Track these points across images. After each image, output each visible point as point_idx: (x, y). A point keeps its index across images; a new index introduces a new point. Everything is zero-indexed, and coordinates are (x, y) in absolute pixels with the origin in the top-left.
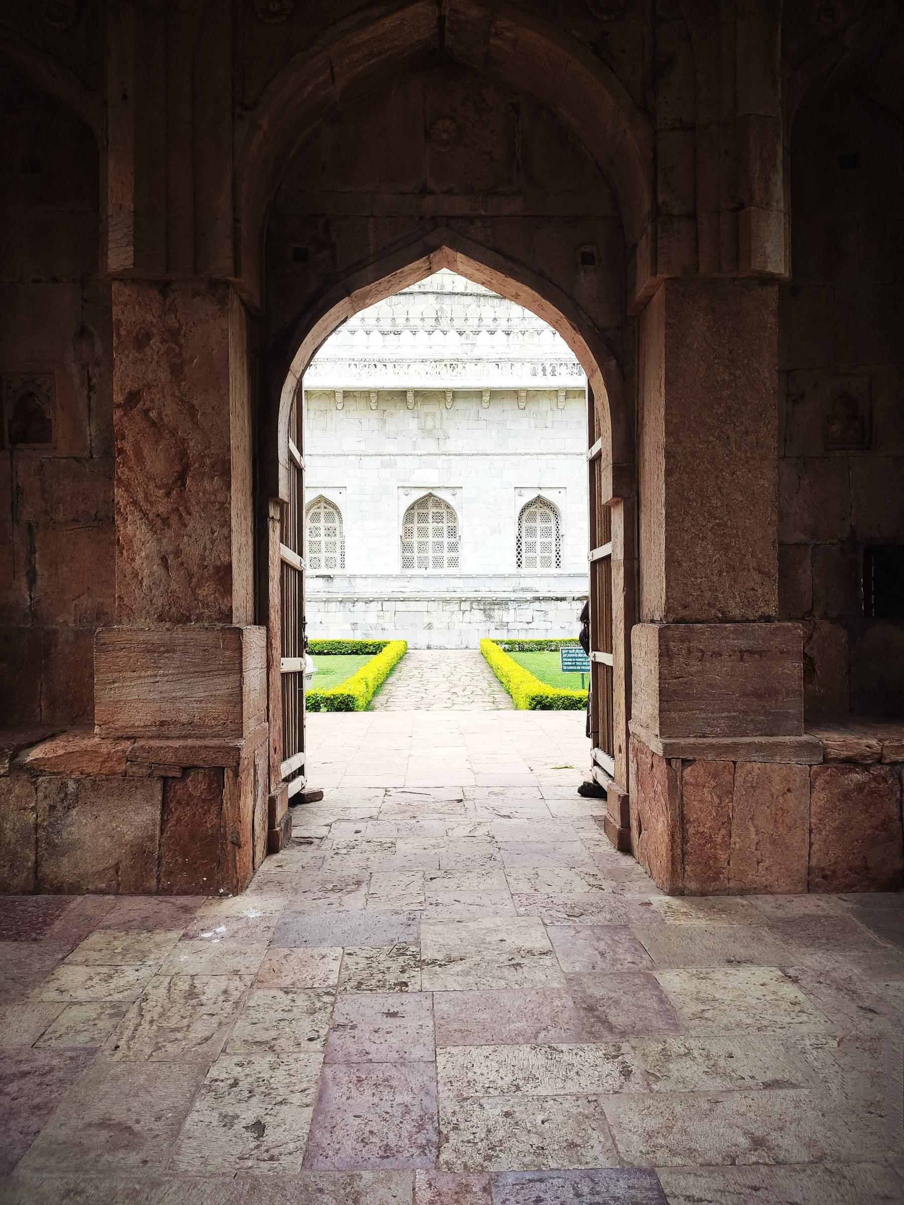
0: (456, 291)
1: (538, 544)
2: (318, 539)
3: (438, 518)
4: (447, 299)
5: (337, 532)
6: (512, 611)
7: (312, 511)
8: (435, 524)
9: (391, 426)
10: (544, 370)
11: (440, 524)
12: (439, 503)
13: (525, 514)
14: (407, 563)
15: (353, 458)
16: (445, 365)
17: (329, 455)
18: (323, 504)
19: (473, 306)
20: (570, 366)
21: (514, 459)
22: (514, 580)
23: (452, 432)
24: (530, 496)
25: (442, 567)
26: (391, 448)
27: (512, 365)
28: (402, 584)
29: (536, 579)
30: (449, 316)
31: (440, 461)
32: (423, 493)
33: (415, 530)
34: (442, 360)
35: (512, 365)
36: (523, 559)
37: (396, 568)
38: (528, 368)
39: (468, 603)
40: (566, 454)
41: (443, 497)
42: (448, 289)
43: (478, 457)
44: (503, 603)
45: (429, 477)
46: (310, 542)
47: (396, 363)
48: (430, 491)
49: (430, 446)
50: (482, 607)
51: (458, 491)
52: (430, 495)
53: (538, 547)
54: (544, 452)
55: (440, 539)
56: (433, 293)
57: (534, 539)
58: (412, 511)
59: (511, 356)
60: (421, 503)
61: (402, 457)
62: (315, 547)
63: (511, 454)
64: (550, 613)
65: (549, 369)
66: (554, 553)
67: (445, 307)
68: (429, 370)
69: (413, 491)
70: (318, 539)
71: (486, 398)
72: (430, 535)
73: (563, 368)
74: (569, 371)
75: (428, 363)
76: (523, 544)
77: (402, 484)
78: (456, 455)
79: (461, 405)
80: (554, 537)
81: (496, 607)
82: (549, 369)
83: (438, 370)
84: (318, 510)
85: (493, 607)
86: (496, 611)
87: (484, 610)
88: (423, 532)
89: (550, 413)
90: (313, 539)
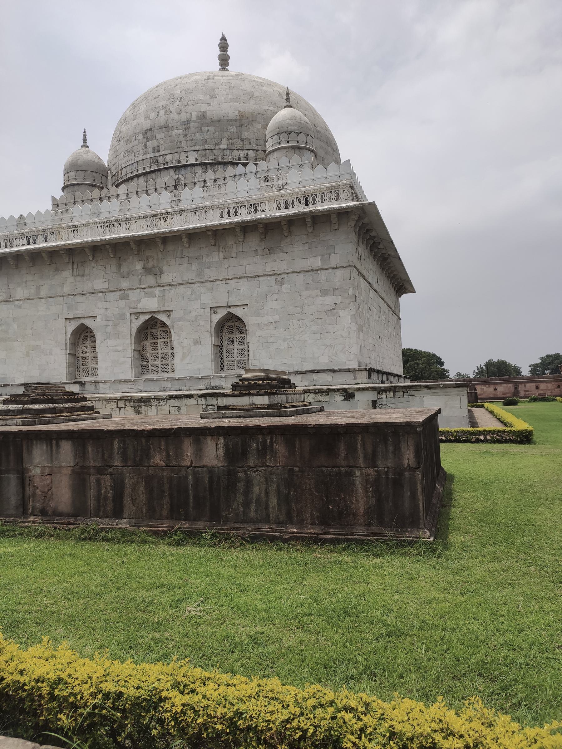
1: (235, 350)
4: (183, 171)
6: (154, 407)
7: (83, 335)
8: (162, 340)
9: (124, 269)
10: (229, 212)
11: (166, 340)
13: (225, 328)
14: (144, 370)
15: (101, 294)
16: (160, 219)
17: (86, 294)
21: (209, 285)
22: (207, 381)
23: (165, 269)
24: (222, 313)
25: (167, 372)
26: (125, 284)
27: (206, 212)
28: (130, 386)
29: (222, 379)
31: (157, 292)
32: (147, 317)
34: (157, 215)
35: (206, 212)
36: (225, 364)
37: (130, 375)
38: (217, 213)
39: (123, 402)
40: (247, 278)
41: (161, 319)
42: (183, 163)
43: (183, 286)
44: (147, 401)
45: (150, 304)
47: (127, 221)
49: (150, 280)
50: (132, 404)
51: (171, 313)
53: (235, 353)
54: (230, 277)
55: (166, 351)
57: (232, 347)
58: (147, 331)
59: (203, 205)
61: (132, 291)
62: (86, 361)
63: (205, 282)
64: (182, 408)
65: (232, 212)
67: (180, 176)
68: (149, 224)
70: (87, 355)
71: (185, 240)
73: (243, 209)
74: (247, 210)
75: (148, 219)
76: (225, 351)
77: (133, 311)
78: (167, 286)
79: (170, 247)
81: (143, 404)
82: (232, 212)
83: (154, 222)
84: (87, 334)
85: (140, 404)
86: (143, 407)
87: (134, 407)
89: (234, 246)
90: (84, 355)
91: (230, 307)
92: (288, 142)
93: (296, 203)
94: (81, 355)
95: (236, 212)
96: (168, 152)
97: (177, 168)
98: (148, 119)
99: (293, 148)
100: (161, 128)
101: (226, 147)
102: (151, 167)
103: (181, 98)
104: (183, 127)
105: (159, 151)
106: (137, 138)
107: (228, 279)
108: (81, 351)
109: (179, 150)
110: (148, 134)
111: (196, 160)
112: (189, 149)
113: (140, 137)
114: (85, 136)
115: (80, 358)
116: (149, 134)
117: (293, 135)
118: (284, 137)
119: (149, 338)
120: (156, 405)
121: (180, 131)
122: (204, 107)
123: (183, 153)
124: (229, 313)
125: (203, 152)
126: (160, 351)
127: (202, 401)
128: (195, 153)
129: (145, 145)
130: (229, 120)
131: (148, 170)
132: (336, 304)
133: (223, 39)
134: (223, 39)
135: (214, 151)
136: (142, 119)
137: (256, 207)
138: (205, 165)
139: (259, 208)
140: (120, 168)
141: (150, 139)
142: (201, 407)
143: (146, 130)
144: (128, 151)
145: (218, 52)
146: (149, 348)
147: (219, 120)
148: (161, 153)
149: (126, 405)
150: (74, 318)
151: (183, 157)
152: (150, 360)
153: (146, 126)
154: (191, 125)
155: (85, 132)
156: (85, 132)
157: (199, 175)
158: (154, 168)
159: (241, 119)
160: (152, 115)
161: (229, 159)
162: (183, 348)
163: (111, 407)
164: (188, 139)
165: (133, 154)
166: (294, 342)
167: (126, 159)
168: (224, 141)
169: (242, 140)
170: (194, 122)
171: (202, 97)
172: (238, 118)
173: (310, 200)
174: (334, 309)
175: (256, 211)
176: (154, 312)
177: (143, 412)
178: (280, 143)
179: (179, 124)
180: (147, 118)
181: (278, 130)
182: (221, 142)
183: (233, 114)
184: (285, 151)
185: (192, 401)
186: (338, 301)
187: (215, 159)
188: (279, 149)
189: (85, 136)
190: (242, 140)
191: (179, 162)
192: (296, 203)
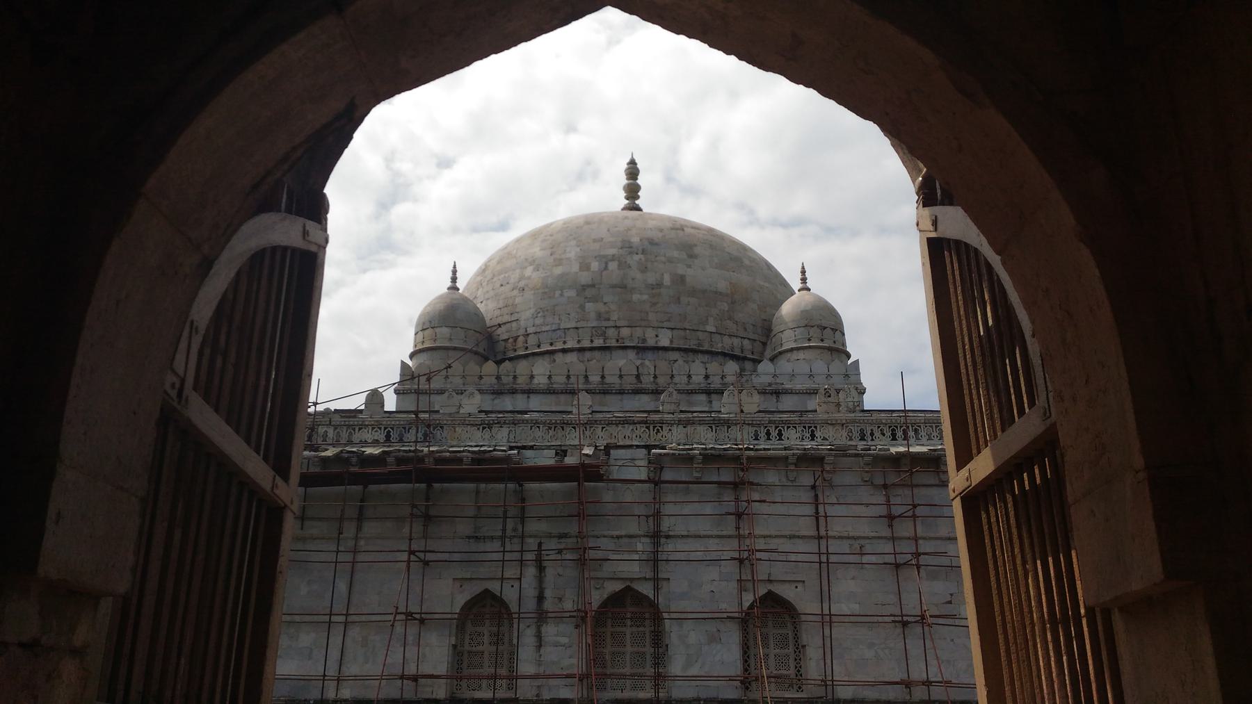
4: (650, 355)
8: (634, 629)
10: (768, 434)
11: (641, 629)
12: (640, 599)
19: (680, 362)
20: (799, 429)
30: (652, 372)
32: (618, 586)
42: (651, 342)
43: (690, 540)
46: (469, 652)
48: (628, 583)
52: (628, 588)
56: (633, 347)
60: (616, 600)
66: (792, 672)
67: (647, 362)
69: (607, 584)
70: (480, 648)
74: (798, 435)
80: (791, 649)
82: (774, 433)
91: (770, 581)
93: (877, 434)
94: (467, 647)
95: (780, 434)
97: (641, 349)
99: (830, 349)
100: (614, 286)
101: (713, 330)
105: (608, 320)
106: (566, 294)
107: (770, 536)
108: (467, 641)
109: (643, 323)
110: (589, 291)
111: (671, 342)
113: (572, 293)
114: (454, 272)
116: (589, 293)
117: (828, 331)
118: (815, 332)
121: (645, 297)
122: (681, 269)
123: (650, 330)
124: (770, 593)
125: (682, 333)
126: (629, 649)
128: (669, 333)
129: (582, 307)
131: (586, 344)
133: (633, 163)
134: (633, 163)
135: (699, 334)
136: (575, 268)
138: (686, 351)
139: (818, 434)
140: (522, 332)
141: (594, 299)
145: (624, 181)
146: (609, 640)
147: (704, 291)
150: (471, 579)
153: (585, 278)
158: (598, 342)
160: (595, 266)
161: (718, 347)
165: (557, 318)
167: (538, 321)
168: (711, 320)
169: (736, 323)
171: (676, 254)
173: (899, 434)
174: (950, 602)
175: (813, 437)
176: (632, 580)
180: (585, 267)
183: (722, 286)
184: (818, 351)
187: (699, 345)
188: (810, 347)
190: (736, 323)
191: (644, 340)
192: (877, 434)
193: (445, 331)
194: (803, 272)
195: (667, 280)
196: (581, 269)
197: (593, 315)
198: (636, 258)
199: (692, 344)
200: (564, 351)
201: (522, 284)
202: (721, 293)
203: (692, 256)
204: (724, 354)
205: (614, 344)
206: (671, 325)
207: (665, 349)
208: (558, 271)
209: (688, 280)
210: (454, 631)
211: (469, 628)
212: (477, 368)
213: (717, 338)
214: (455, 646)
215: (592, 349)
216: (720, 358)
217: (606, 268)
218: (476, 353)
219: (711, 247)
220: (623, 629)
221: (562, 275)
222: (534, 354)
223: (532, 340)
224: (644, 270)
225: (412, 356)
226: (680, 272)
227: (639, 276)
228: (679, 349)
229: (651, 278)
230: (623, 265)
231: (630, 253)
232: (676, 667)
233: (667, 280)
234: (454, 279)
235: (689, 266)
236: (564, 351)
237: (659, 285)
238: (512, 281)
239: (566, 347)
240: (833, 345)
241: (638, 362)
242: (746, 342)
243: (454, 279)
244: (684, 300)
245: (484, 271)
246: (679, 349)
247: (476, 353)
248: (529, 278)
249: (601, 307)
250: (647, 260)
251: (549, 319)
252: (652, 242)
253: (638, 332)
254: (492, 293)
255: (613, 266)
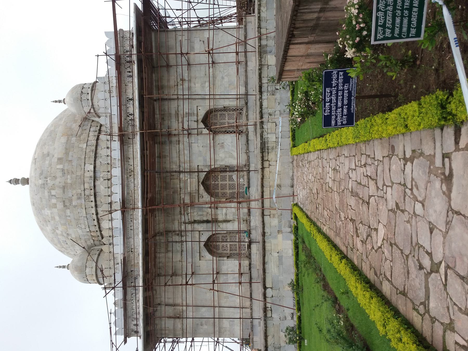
0: (93, 169)
2: (228, 246)
3: (216, 178)
4: (98, 174)
5: (225, 235)
8: (219, 180)
11: (219, 177)
12: (207, 178)
18: (210, 244)
19: (100, 160)
30: (106, 173)
32: (202, 188)
33: (222, 191)
42: (92, 174)
46: (230, 251)
48: (200, 183)
52: (203, 183)
56: (94, 182)
60: (207, 189)
62: (233, 248)
64: (269, 112)
67: (101, 175)
70: (228, 246)
72: (225, 182)
76: (229, 130)
88: (223, 187)
92: (88, 94)
94: (228, 252)
96: (82, 186)
98: (56, 204)
99: (92, 90)
102: (92, 201)
103: (45, 178)
104: (66, 174)
106: (69, 214)
108: (225, 252)
109: (82, 177)
111: (91, 164)
112: (83, 170)
113: (68, 211)
114: (60, 267)
115: (231, 252)
117: (83, 91)
119: (216, 191)
120: (268, 134)
121: (69, 176)
122: (55, 160)
125: (86, 159)
126: (227, 182)
127: (265, 96)
128: (86, 165)
129: (75, 206)
130: (67, 143)
131: (93, 204)
132: (200, 41)
135: (87, 151)
136: (55, 210)
137: (129, 99)
138: (95, 157)
140: (89, 234)
141: (71, 201)
142: (270, 97)
143: (64, 206)
144: (77, 224)
146: (225, 191)
147: (66, 149)
148: (83, 193)
149: (267, 160)
151: (87, 174)
152: (234, 191)
154: (66, 168)
155: (57, 267)
156: (57, 267)
157: (103, 160)
158: (92, 198)
159: (68, 135)
160: (54, 201)
161: (95, 142)
162: (226, 157)
163: (269, 173)
164: (75, 170)
166: (225, 71)
167: (83, 227)
168: (81, 146)
170: (64, 166)
171: (47, 162)
172: (66, 137)
174: (204, 42)
176: (199, 182)
177: (272, 145)
178: (88, 100)
179: (63, 178)
180: (55, 206)
181: (79, 101)
182: (82, 148)
183: (63, 140)
185: (265, 104)
186: (198, 39)
189: (60, 267)
191: (91, 177)
193: (88, 270)
194: (56, 102)
195: (60, 166)
196: (56, 207)
197: (79, 201)
198: (49, 181)
199: (93, 155)
200: (97, 214)
201: (65, 235)
202: (67, 141)
203: (48, 155)
204: (98, 139)
205: (93, 191)
206: (83, 164)
207: (95, 167)
208: (57, 218)
209: (59, 157)
210: (222, 258)
211: (220, 251)
212: (106, 254)
213: (89, 143)
214: (228, 257)
215: (96, 201)
216: (99, 141)
217: (55, 196)
218: (99, 255)
219: (45, 144)
220: (220, 185)
221: (60, 217)
222: (99, 228)
223: (93, 229)
224: (55, 177)
225: (101, 284)
226: (56, 160)
227: (58, 180)
228: (95, 161)
229: (59, 174)
230: (53, 188)
231: (47, 184)
232: (234, 162)
233: (60, 166)
234: (64, 267)
235: (53, 156)
236: (97, 214)
237: (63, 170)
238: (64, 239)
239: (95, 213)
240: (90, 89)
241: (102, 180)
242: (92, 129)
243: (64, 267)
244: (70, 158)
245: (61, 251)
246: (95, 161)
247: (99, 255)
248: (62, 232)
249: (75, 197)
250: (51, 176)
251: (82, 222)
252: (41, 174)
253: (87, 180)
254: (71, 248)
255: (53, 192)
